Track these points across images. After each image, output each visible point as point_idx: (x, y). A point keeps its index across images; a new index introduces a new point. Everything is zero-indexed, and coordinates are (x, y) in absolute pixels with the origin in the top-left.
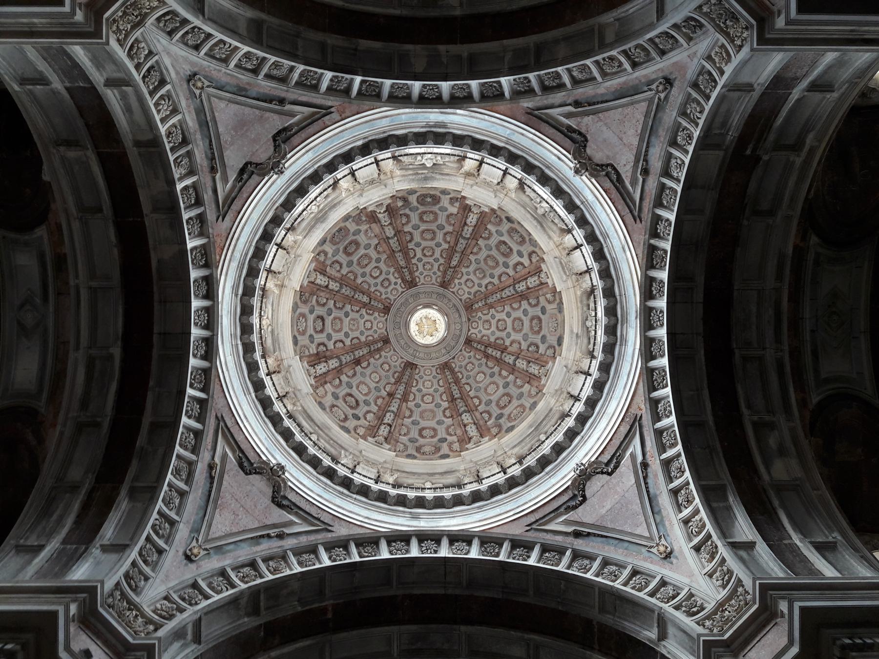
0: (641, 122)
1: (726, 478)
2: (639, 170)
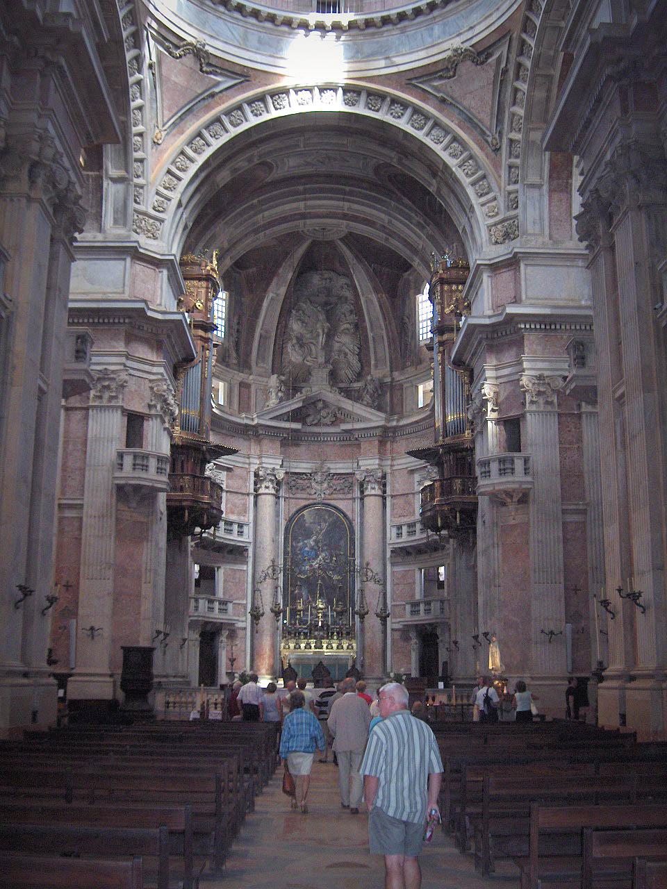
0: (477, 115)
1: (214, 165)
2: (445, 97)
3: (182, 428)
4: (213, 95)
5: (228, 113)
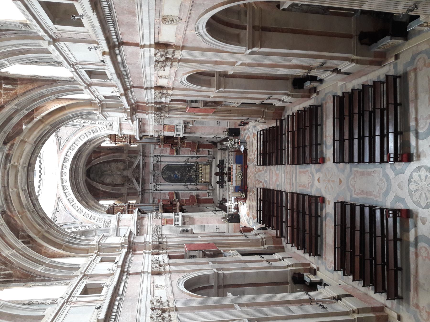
3: (158, 210)
4: (65, 208)
5: (70, 203)
